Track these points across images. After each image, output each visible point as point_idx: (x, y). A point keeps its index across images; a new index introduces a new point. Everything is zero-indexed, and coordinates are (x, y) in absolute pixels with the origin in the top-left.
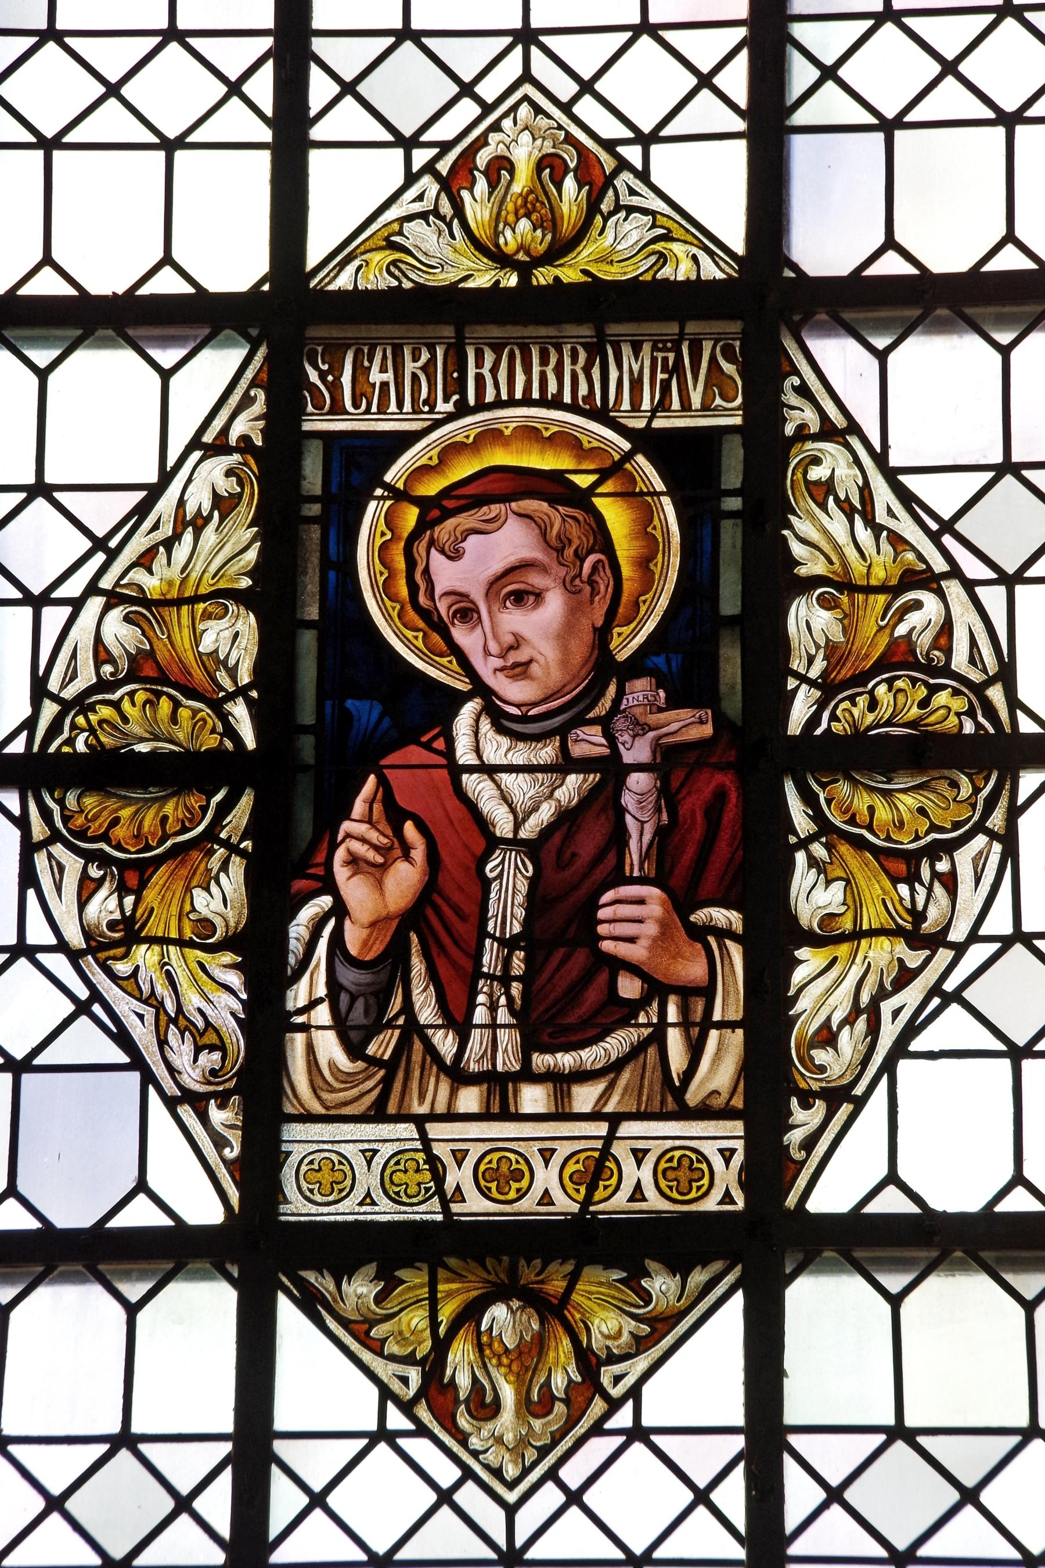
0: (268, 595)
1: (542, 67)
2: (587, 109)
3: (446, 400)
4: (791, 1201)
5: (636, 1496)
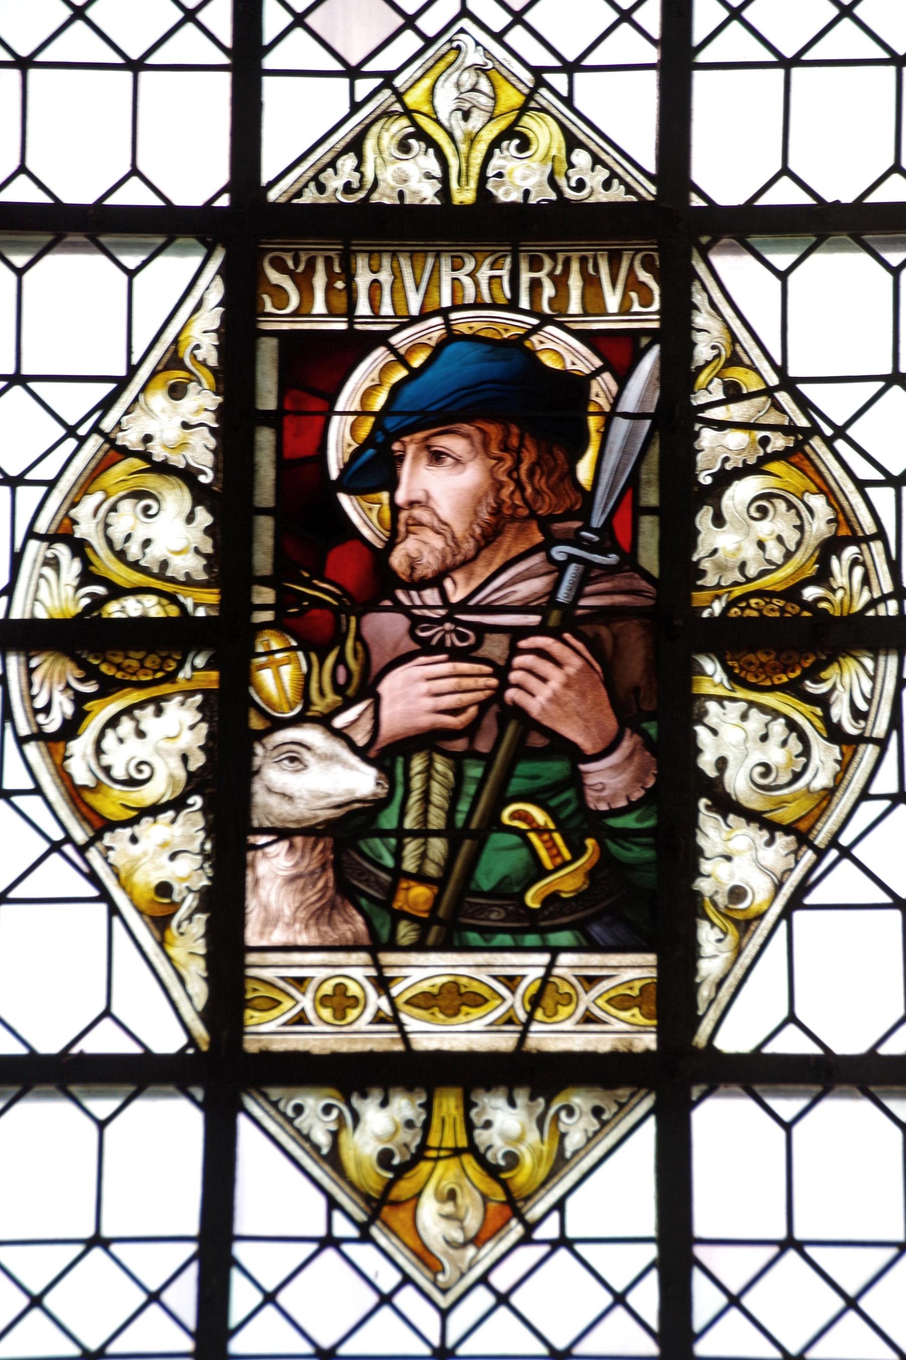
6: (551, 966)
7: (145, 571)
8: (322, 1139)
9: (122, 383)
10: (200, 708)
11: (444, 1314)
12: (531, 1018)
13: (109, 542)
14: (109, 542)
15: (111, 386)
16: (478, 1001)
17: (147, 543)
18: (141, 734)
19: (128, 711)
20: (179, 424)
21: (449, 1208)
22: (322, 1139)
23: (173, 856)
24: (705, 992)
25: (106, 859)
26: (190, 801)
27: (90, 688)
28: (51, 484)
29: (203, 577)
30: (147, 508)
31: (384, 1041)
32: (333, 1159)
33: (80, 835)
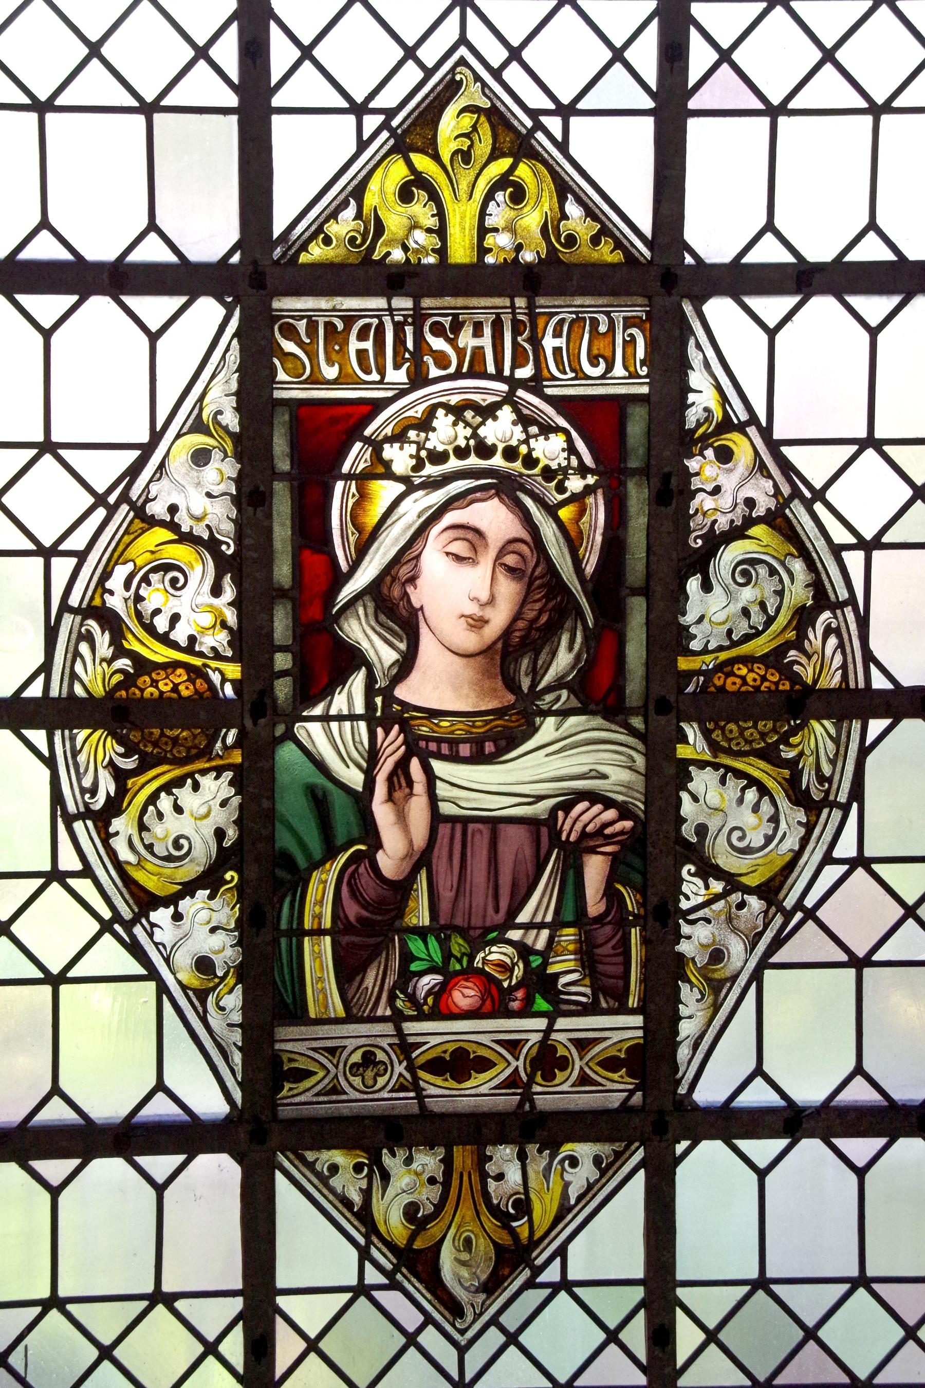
3: (397, 367)
4: (682, 1090)
7: (174, 645)
8: (356, 1198)
9: (146, 450)
10: (231, 783)
12: (531, 1079)
13: (139, 615)
14: (139, 615)
15: (136, 454)
17: (175, 619)
18: (178, 809)
19: (167, 788)
20: (201, 492)
21: (465, 1256)
22: (356, 1198)
23: (213, 930)
24: (683, 1053)
25: (151, 935)
26: (228, 876)
27: (129, 764)
28: (81, 556)
29: (229, 654)
30: (174, 581)
31: (406, 1102)
32: (364, 1215)
33: (127, 914)
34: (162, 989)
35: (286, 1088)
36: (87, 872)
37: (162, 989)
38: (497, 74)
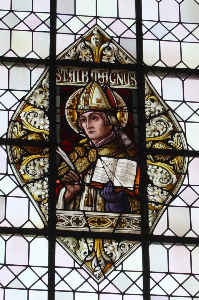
0: (50, 113)
1: (99, 22)
2: (107, 30)
5: (122, 282)
6: (120, 216)
11: (98, 284)
16: (105, 222)
24: (150, 224)
34: (30, 200)
35: (58, 223)
36: (14, 174)
37: (30, 200)
38: (104, 30)
